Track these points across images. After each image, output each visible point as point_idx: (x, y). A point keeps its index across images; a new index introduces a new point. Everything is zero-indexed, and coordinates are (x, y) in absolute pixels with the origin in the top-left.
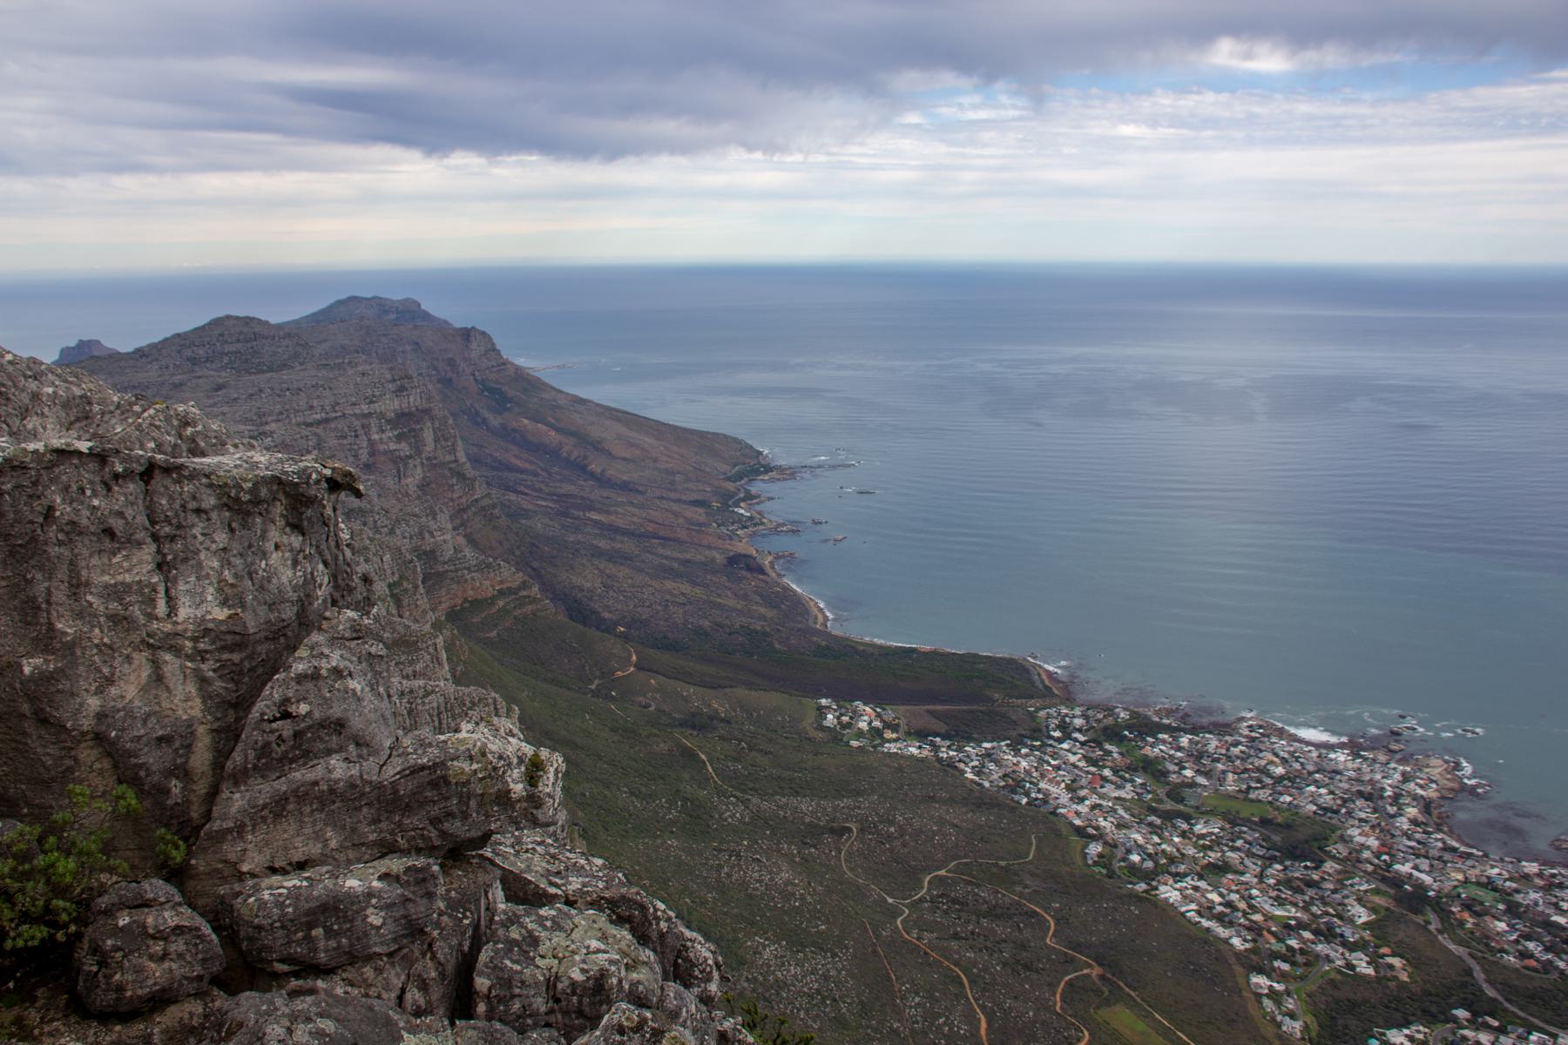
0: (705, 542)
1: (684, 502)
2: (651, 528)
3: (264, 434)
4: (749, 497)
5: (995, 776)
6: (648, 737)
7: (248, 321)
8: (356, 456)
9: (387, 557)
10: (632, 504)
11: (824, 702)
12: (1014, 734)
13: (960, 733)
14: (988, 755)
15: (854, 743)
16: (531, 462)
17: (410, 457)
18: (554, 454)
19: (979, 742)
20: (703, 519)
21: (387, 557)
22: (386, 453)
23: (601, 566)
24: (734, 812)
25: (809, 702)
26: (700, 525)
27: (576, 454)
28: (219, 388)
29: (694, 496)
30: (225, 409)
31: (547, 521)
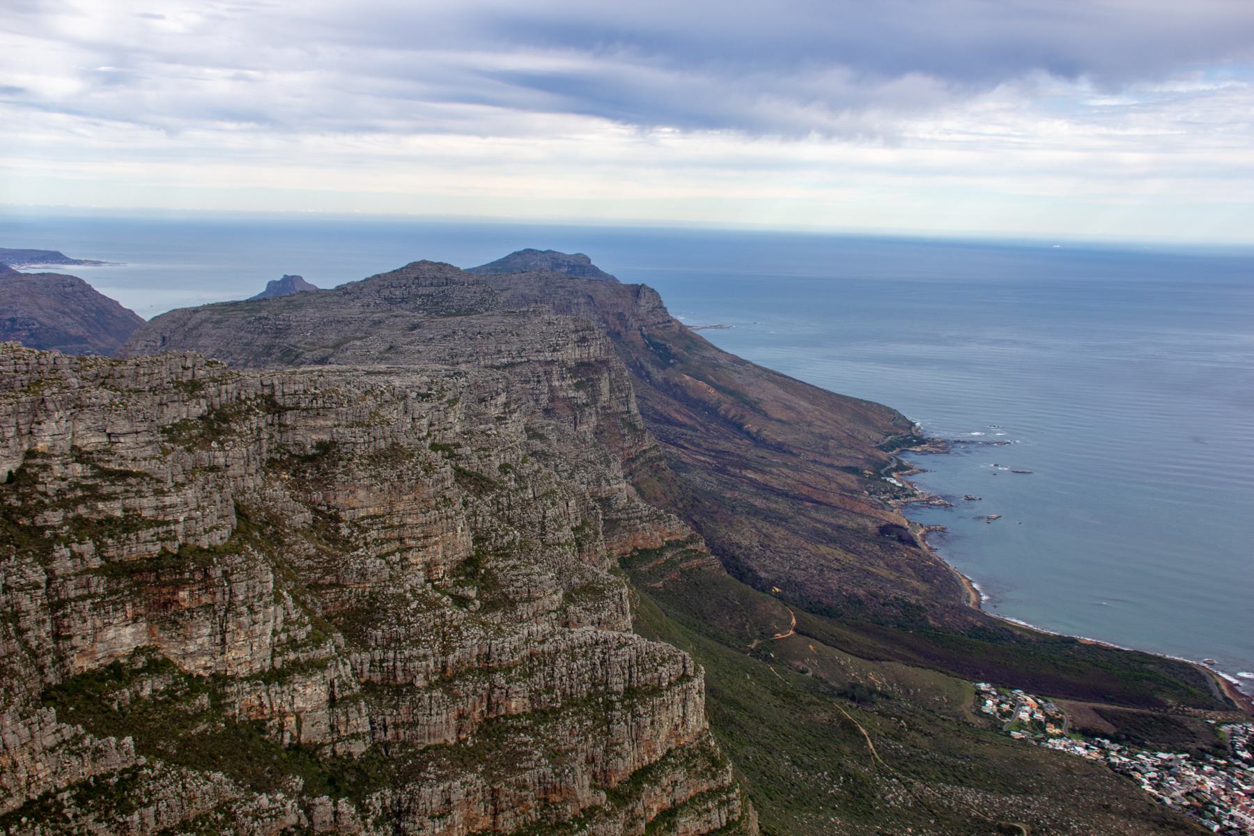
0: (857, 510)
1: (838, 468)
2: (805, 491)
3: (458, 374)
4: (901, 468)
5: (1177, 793)
6: (809, 704)
7: (441, 266)
8: (537, 400)
9: (572, 503)
11: (983, 686)
12: (1193, 747)
13: (1131, 737)
14: (1165, 767)
15: (1016, 735)
16: (691, 417)
17: (587, 405)
18: (711, 411)
19: (1153, 751)
20: (855, 486)
21: (572, 503)
22: (564, 399)
23: (759, 525)
24: (896, 796)
25: (968, 685)
26: (852, 491)
27: (732, 413)
28: (414, 327)
29: (847, 463)
30: (421, 348)
31: (705, 475)
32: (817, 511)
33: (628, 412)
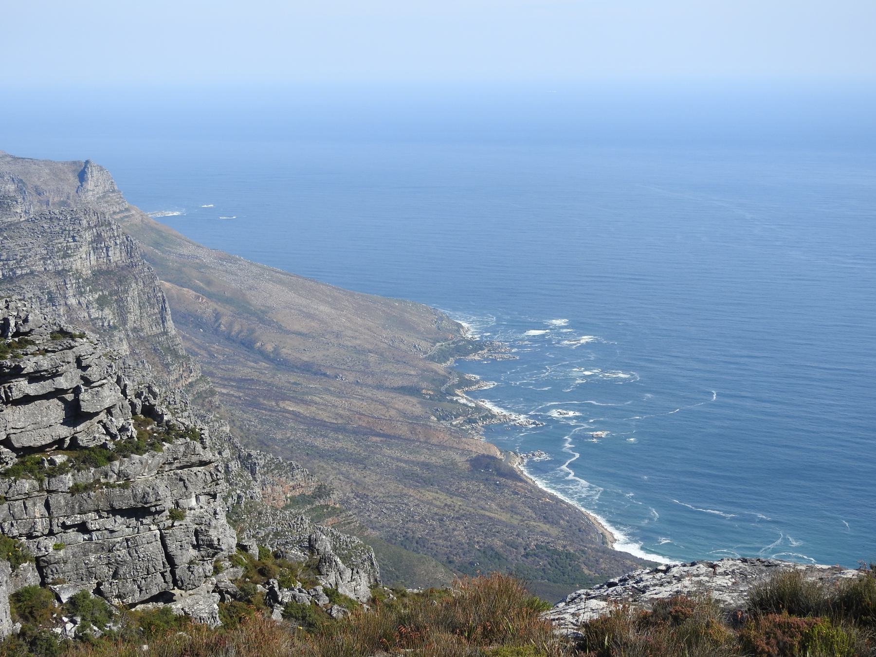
0: (434, 441)
10: (327, 390)
17: (115, 328)
18: (209, 328)
23: (344, 469)
27: (236, 328)
29: (399, 382)
32: (390, 446)
33: (165, 333)
